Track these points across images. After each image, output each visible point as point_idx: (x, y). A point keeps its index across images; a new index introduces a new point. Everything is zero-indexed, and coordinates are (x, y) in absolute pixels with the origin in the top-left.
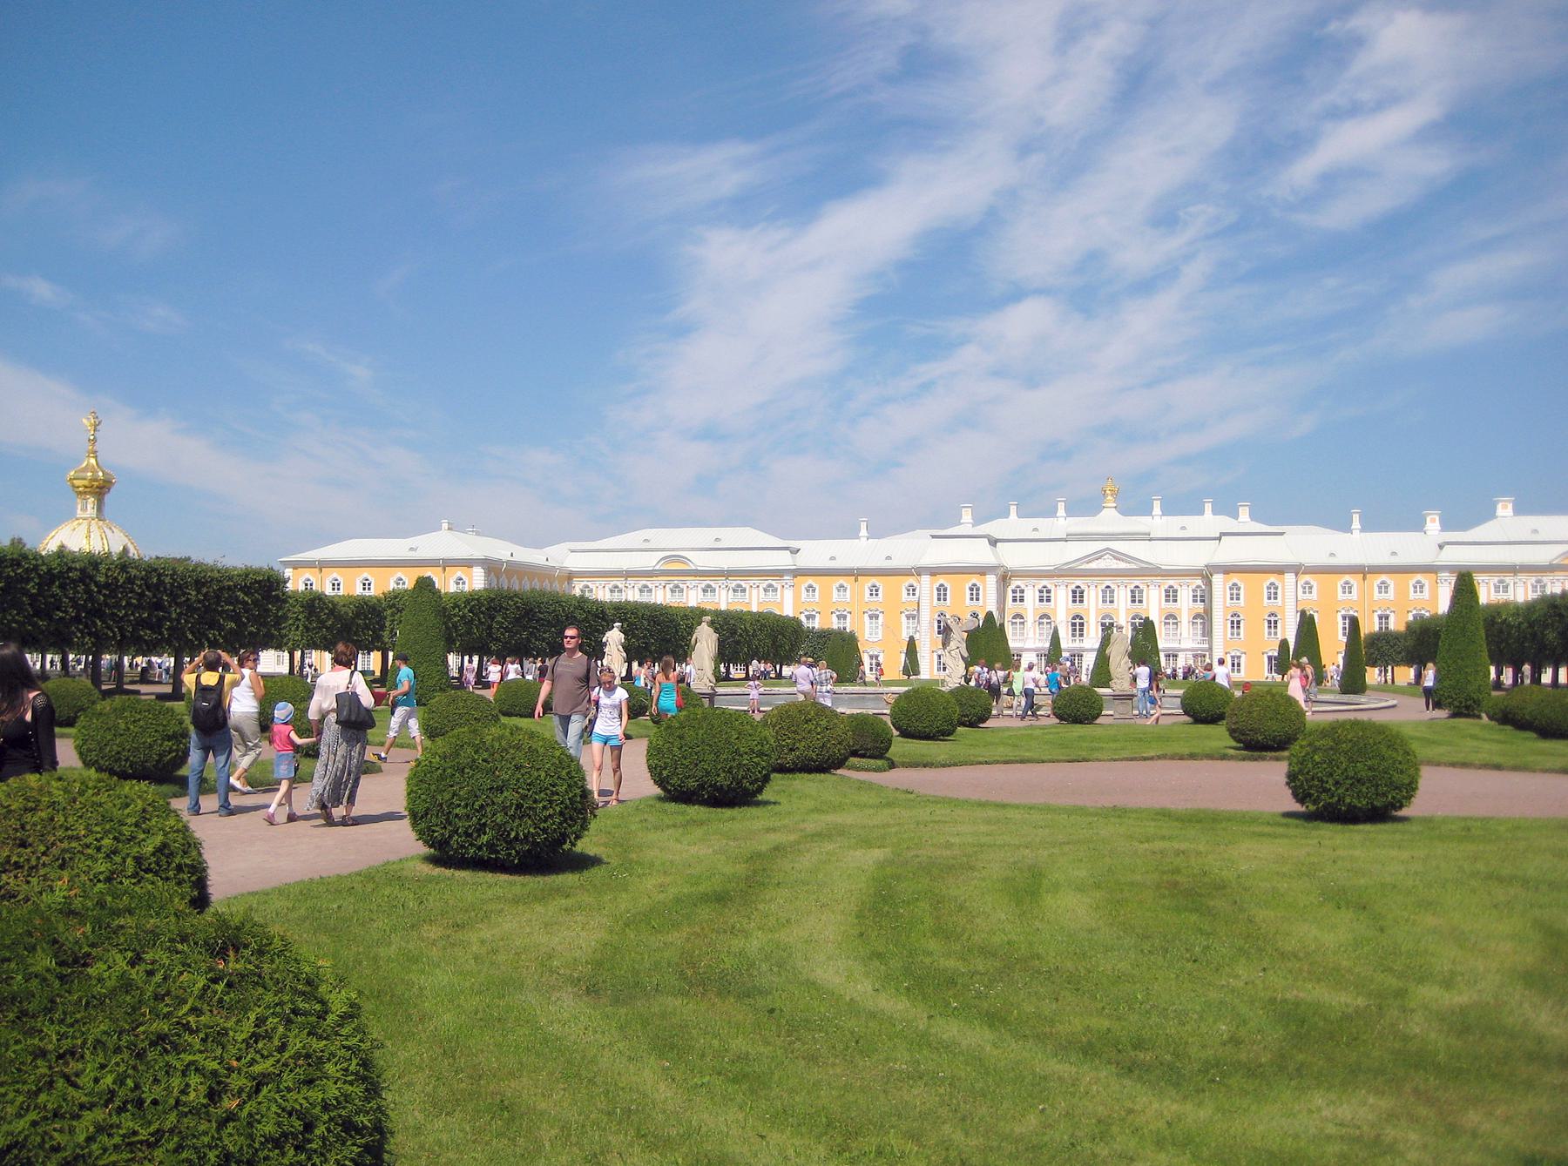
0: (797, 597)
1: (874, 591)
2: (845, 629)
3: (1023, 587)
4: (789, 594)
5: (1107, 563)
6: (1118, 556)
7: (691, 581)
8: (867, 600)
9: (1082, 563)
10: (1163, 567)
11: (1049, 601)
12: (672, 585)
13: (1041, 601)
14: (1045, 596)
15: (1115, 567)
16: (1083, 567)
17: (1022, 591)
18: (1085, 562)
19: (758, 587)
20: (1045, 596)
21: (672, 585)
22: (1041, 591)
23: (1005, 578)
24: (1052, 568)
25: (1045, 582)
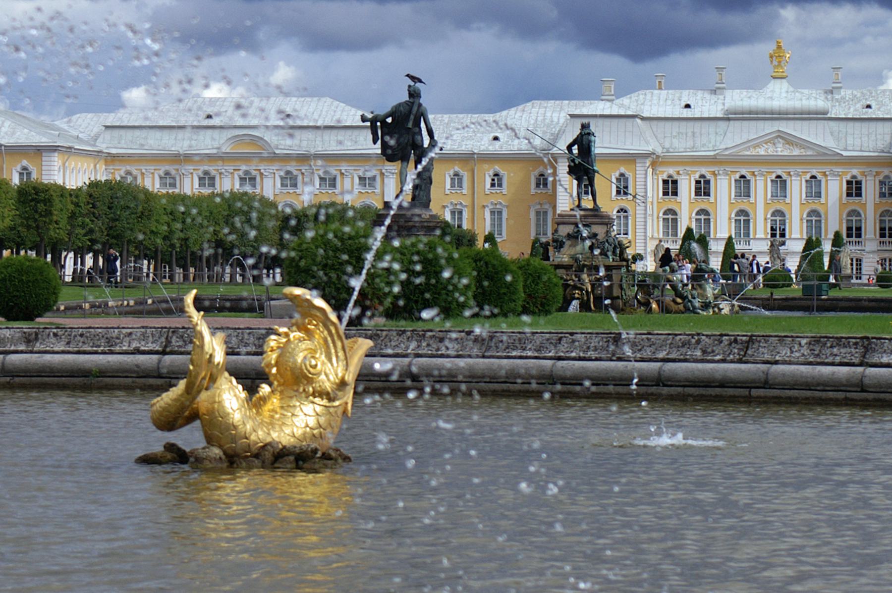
1: (496, 180)
2: (460, 226)
3: (675, 177)
5: (781, 150)
6: (789, 140)
9: (748, 149)
10: (845, 153)
11: (707, 194)
13: (698, 193)
14: (703, 188)
15: (785, 153)
16: (748, 153)
17: (675, 182)
18: (749, 147)
20: (703, 188)
21: (241, 173)
22: (698, 182)
23: (656, 161)
24: (712, 153)
25: (704, 170)
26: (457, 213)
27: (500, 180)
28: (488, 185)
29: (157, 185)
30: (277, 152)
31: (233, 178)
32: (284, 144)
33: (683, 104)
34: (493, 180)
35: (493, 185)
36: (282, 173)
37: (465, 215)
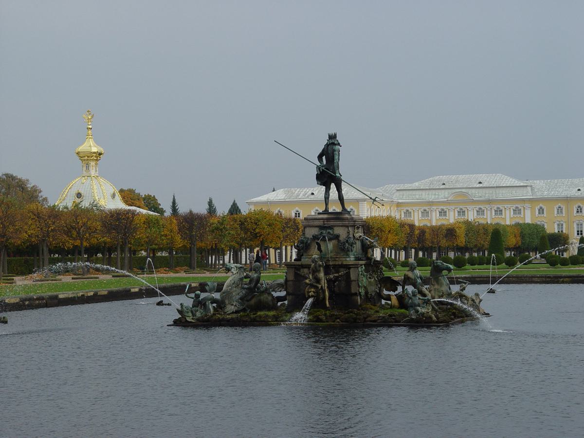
0: (533, 214)
4: (528, 213)
7: (470, 207)
8: (575, 215)
12: (458, 209)
19: (510, 208)
21: (458, 209)
26: (560, 225)
27: (581, 209)
28: (575, 212)
29: (403, 216)
30: (474, 199)
31: (454, 212)
32: (477, 195)
33: (478, 182)
34: (578, 209)
35: (578, 212)
36: (477, 209)
37: (564, 226)
